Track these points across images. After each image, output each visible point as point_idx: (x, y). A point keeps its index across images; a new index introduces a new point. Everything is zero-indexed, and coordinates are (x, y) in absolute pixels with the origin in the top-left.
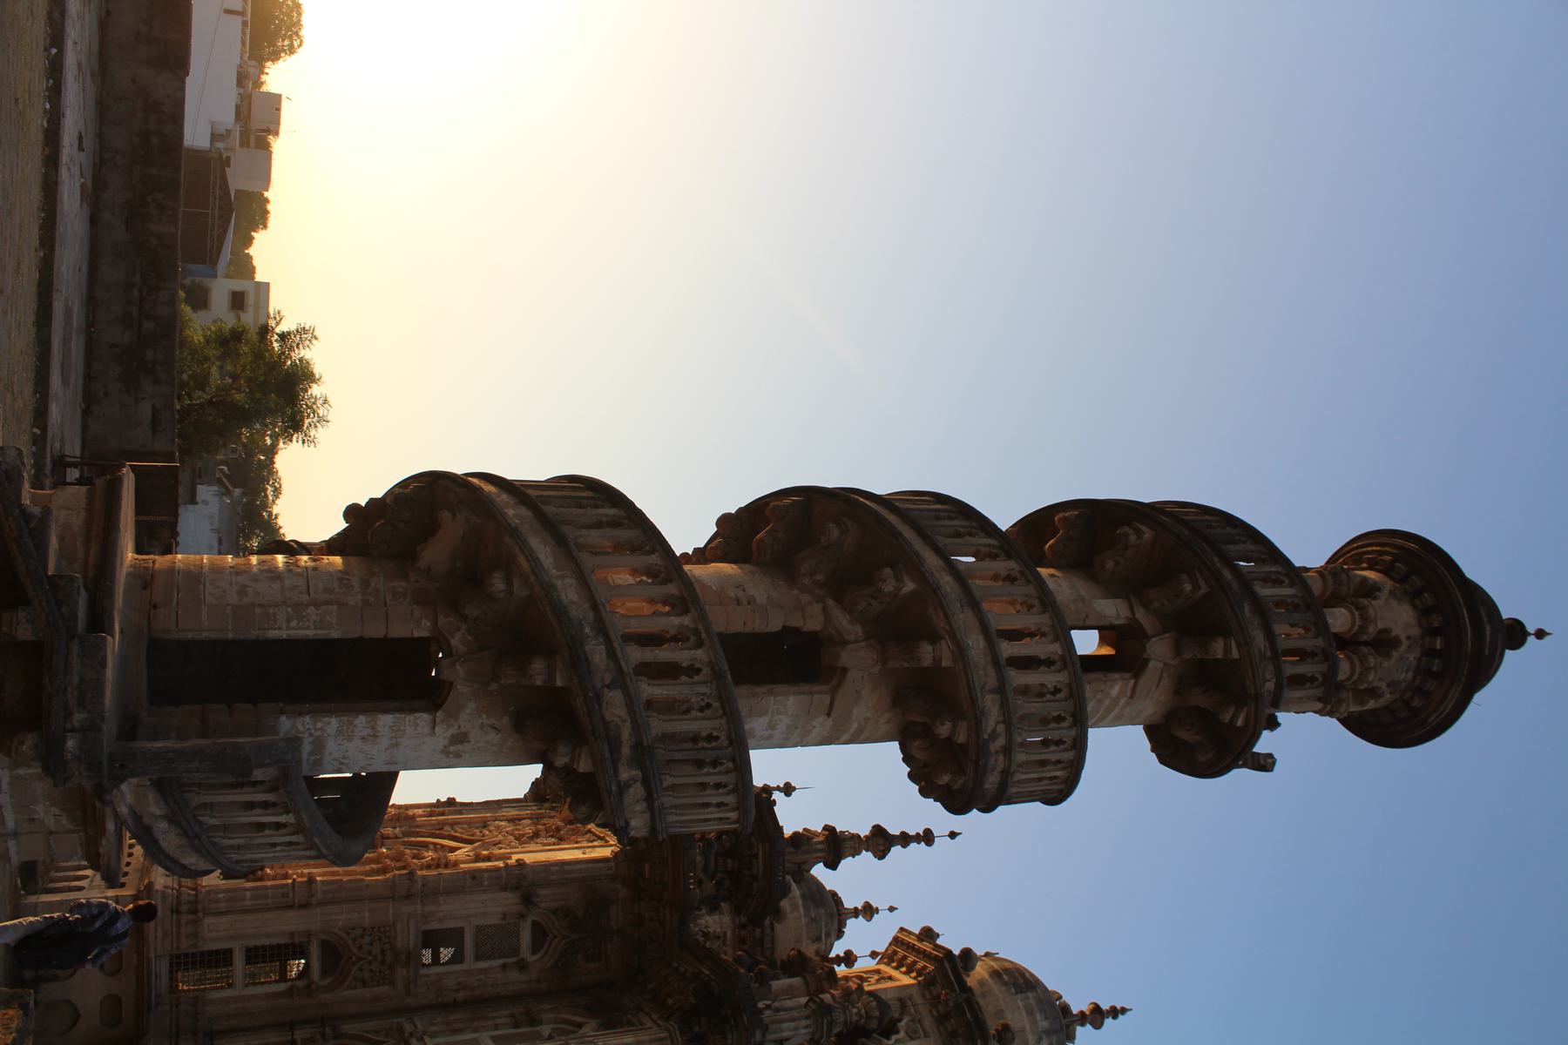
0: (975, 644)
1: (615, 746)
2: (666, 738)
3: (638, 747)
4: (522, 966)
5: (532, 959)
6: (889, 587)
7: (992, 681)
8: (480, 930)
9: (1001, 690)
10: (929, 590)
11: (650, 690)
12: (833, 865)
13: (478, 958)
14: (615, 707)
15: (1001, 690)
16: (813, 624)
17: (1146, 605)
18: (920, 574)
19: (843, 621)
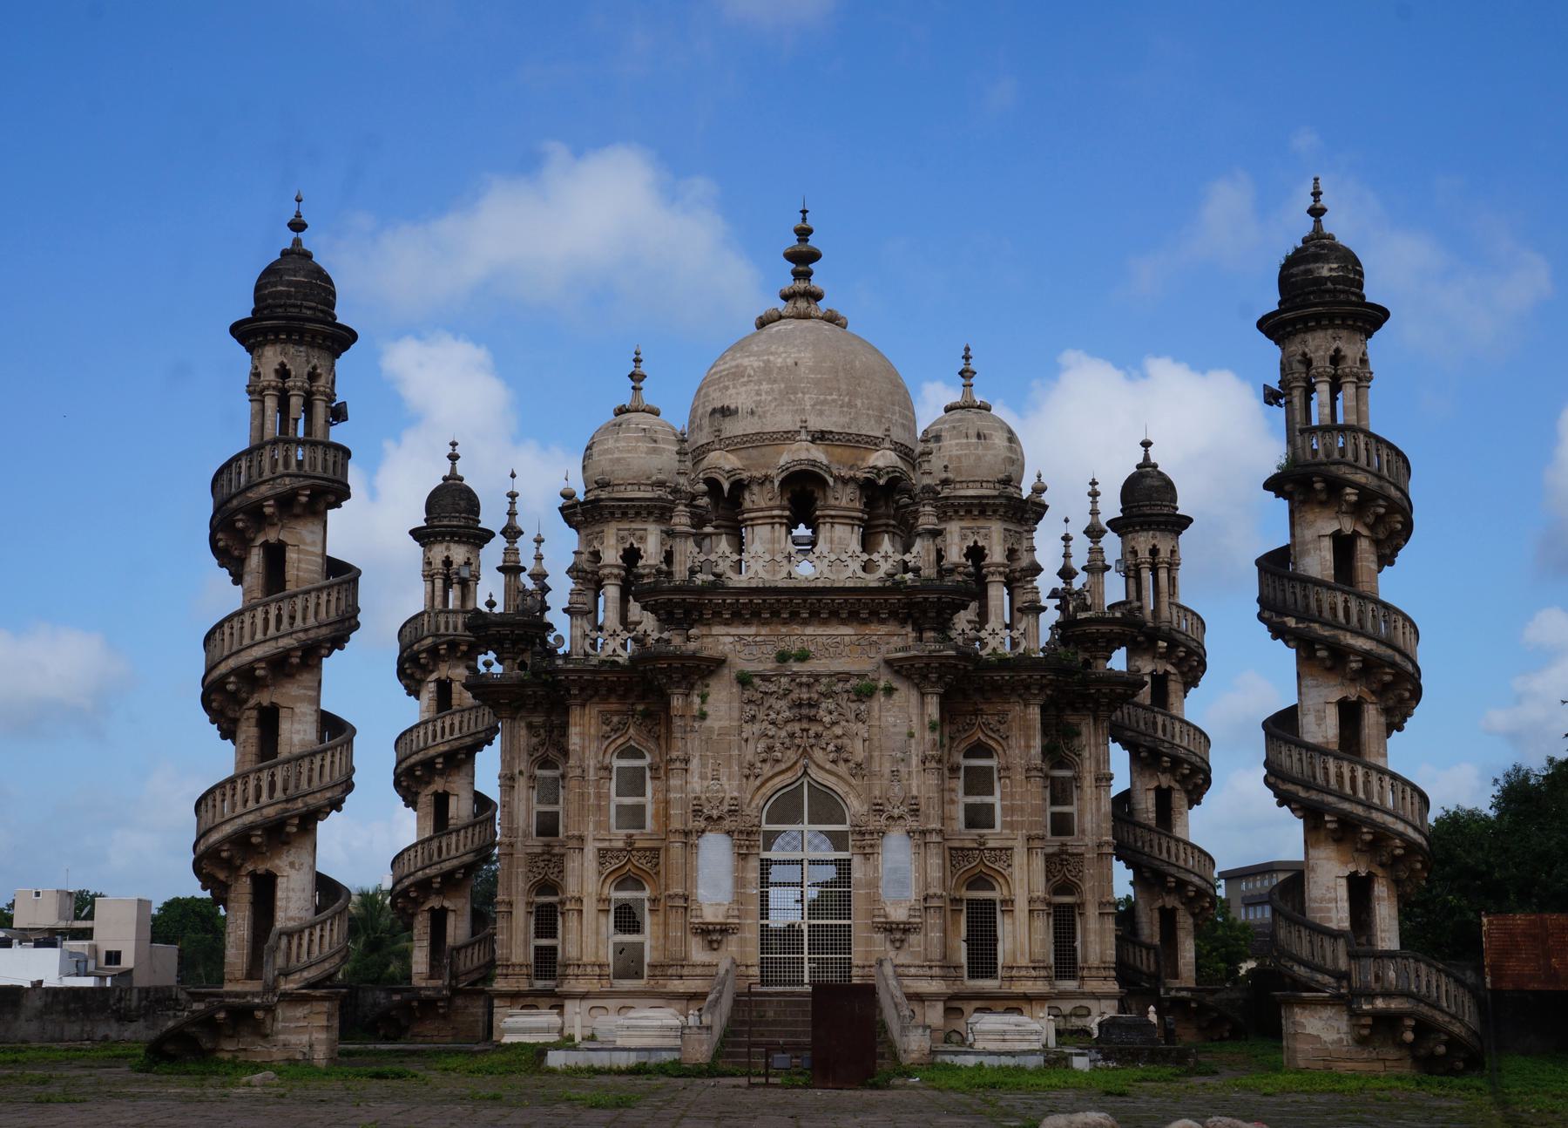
0: (257, 652)
1: (287, 810)
2: (285, 790)
3: (287, 801)
4: (563, 777)
5: (561, 771)
6: (231, 687)
7: (273, 643)
8: (540, 802)
9: (276, 638)
10: (233, 671)
11: (264, 798)
12: (524, 569)
13: (557, 803)
14: (270, 812)
15: (276, 638)
16: (254, 713)
17: (253, 540)
18: (227, 675)
19: (252, 702)
